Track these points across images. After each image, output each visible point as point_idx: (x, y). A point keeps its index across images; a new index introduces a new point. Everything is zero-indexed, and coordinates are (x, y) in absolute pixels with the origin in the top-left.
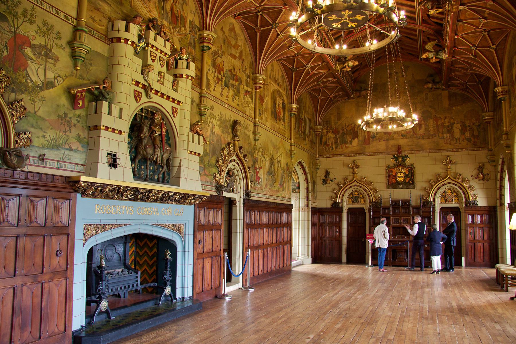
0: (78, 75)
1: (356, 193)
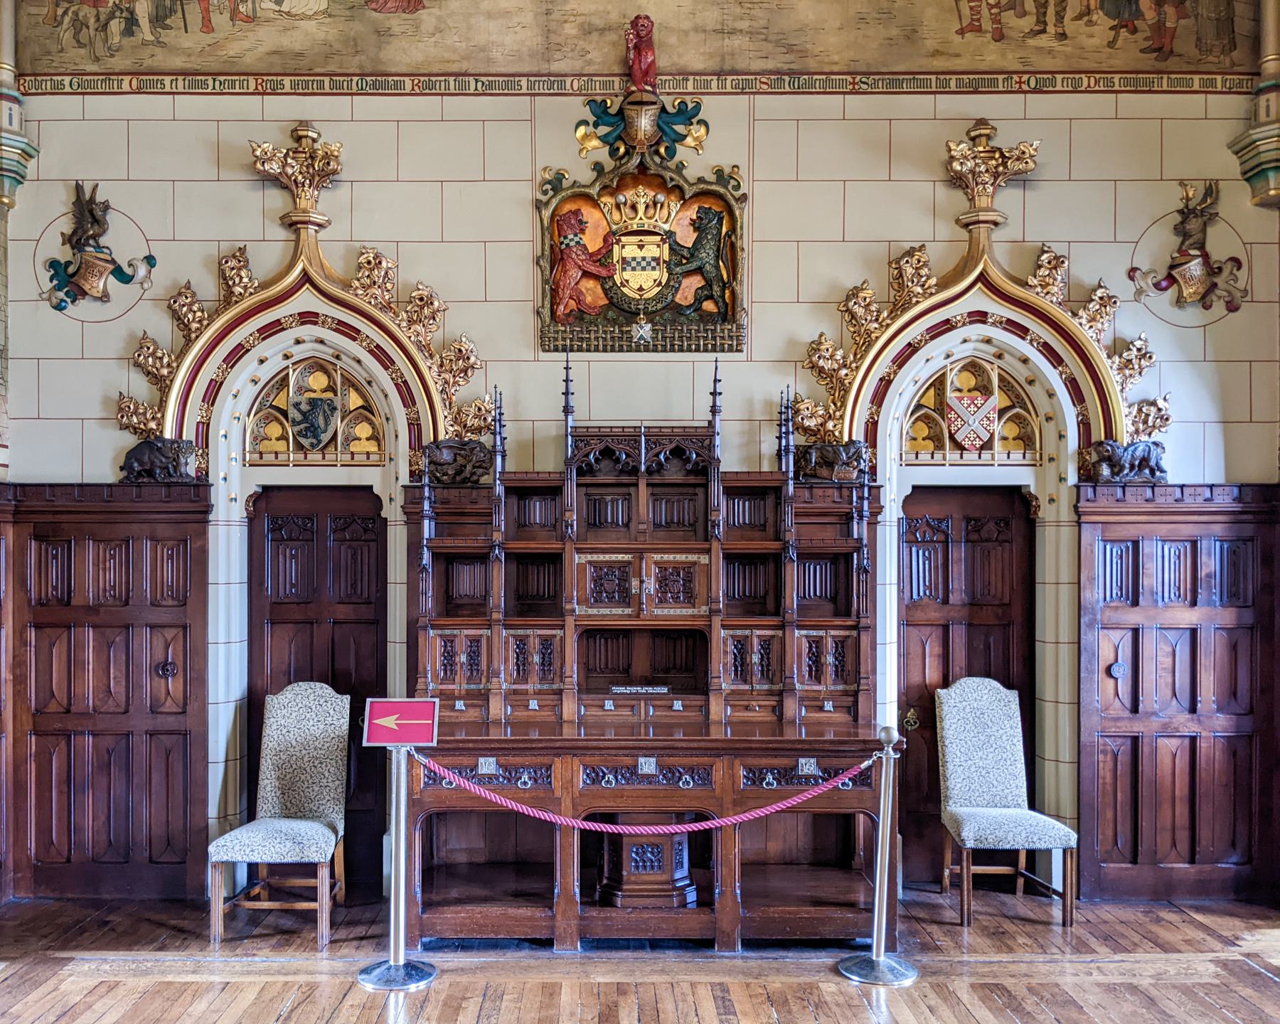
1: (318, 381)
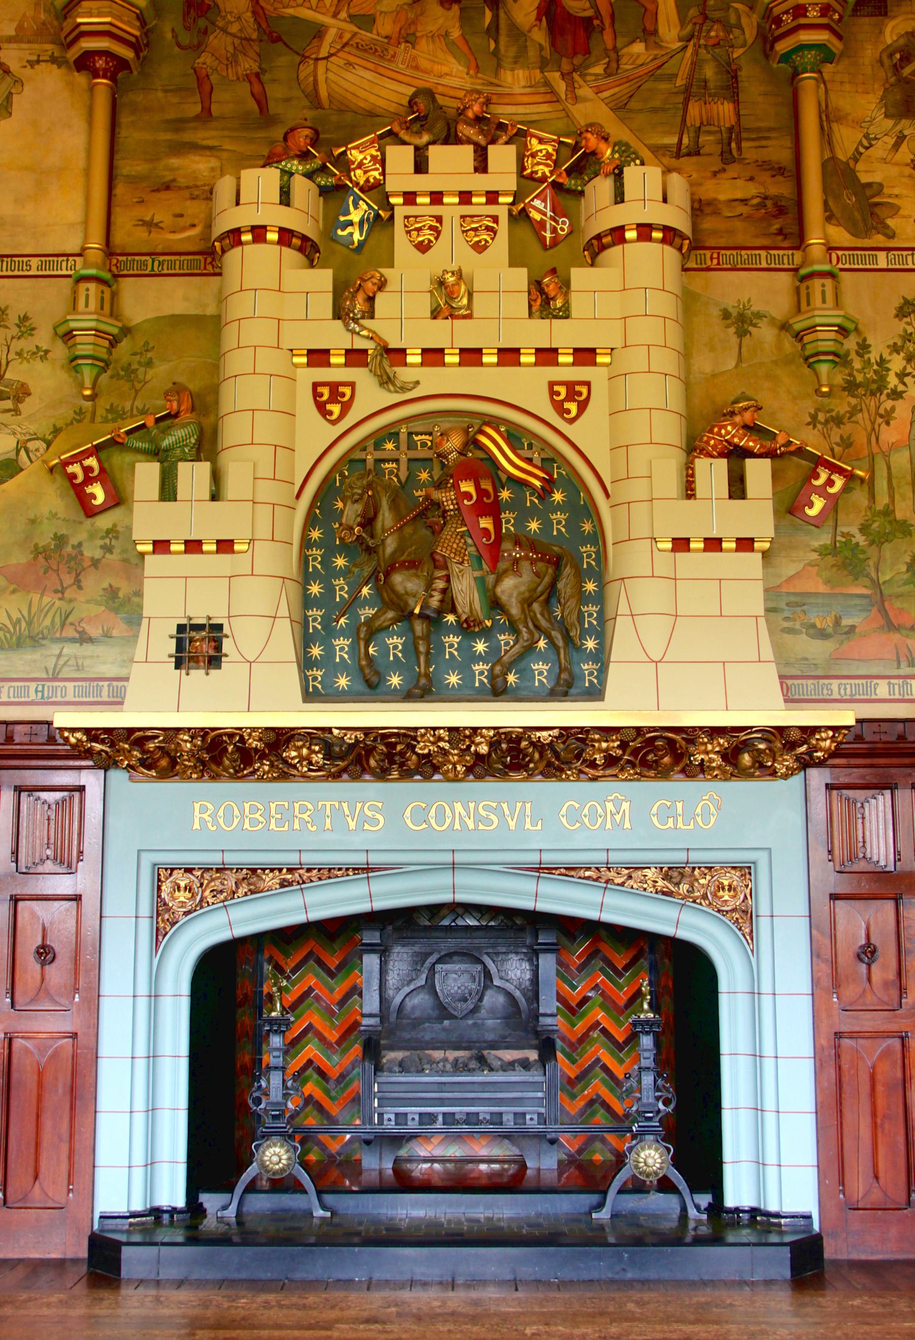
0: (100, 412)
